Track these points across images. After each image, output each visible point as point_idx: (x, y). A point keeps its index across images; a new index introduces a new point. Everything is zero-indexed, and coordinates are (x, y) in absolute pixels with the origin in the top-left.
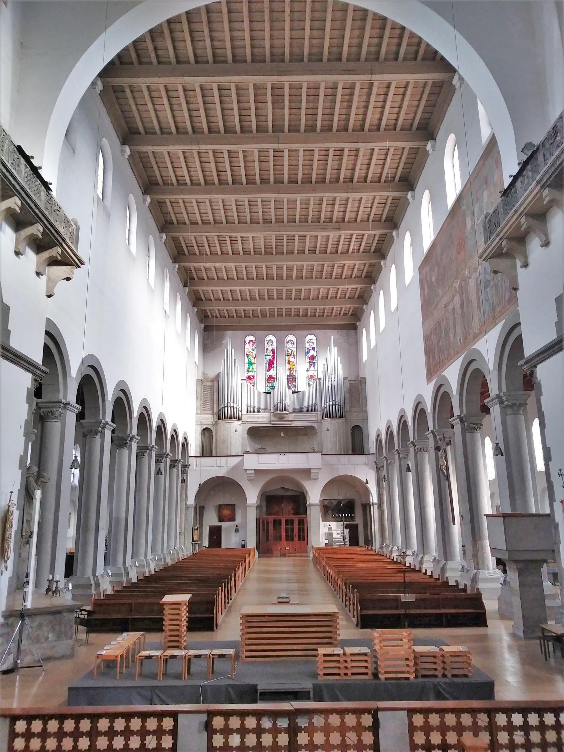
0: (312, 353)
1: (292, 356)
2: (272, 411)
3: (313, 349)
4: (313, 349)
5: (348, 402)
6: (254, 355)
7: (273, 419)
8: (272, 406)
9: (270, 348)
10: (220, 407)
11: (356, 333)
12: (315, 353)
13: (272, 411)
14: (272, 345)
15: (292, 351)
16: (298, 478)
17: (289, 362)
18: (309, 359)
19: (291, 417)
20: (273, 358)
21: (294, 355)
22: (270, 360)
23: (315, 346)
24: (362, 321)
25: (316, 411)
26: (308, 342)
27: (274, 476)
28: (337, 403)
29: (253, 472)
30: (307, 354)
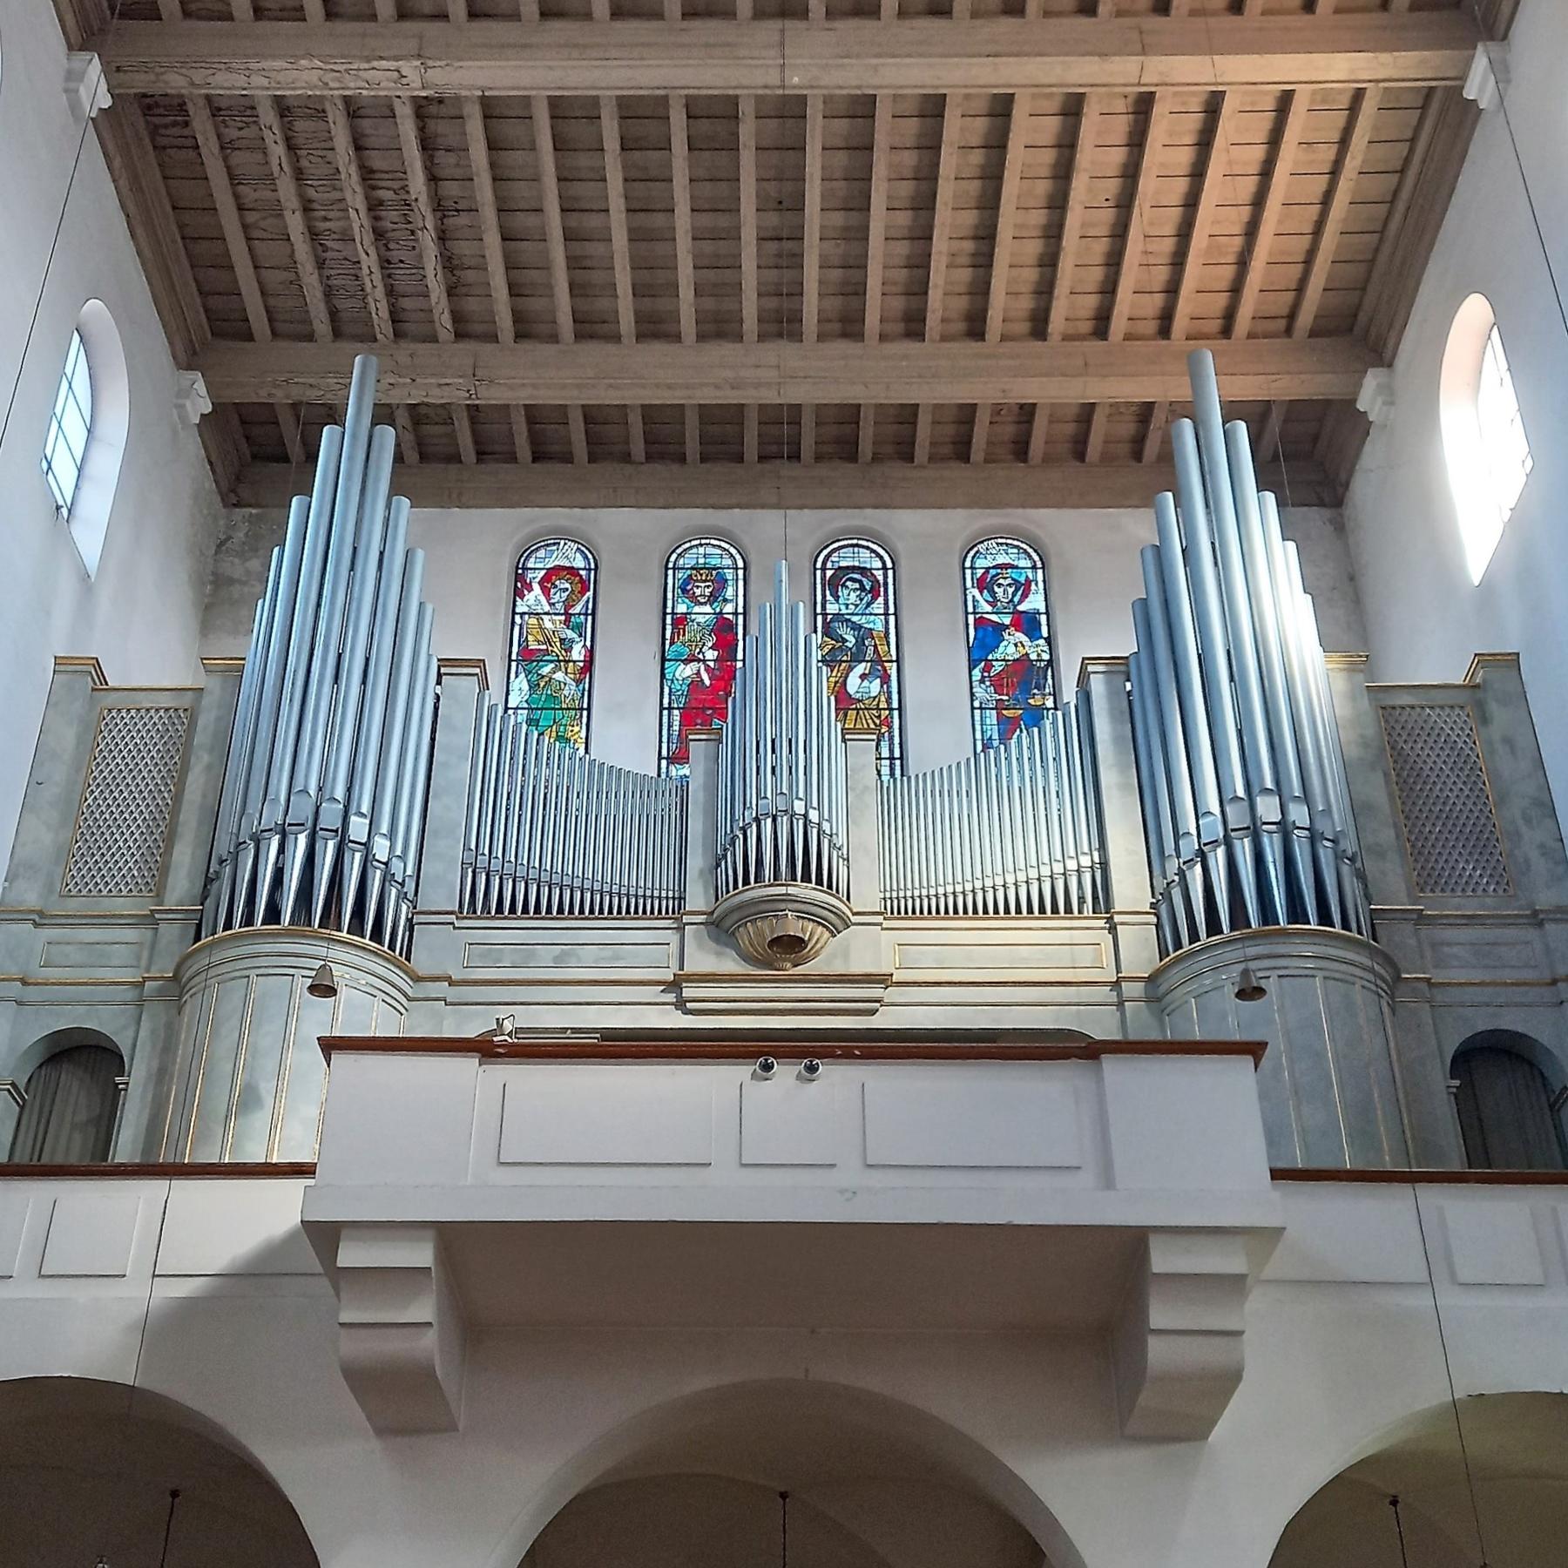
0: (1012, 646)
1: (861, 668)
2: (697, 898)
3: (1027, 624)
4: (1027, 624)
5: (1387, 836)
6: (578, 653)
7: (702, 959)
8: (696, 861)
9: (703, 614)
10: (223, 846)
11: (1340, 528)
12: (1036, 650)
13: (697, 898)
14: (712, 599)
15: (863, 634)
16: (962, 1405)
17: (844, 701)
18: (998, 684)
19: (862, 949)
20: (725, 675)
21: (878, 661)
22: (695, 684)
23: (1035, 602)
24: (1400, 363)
25: (1103, 899)
26: (982, 584)
27: (700, 1382)
28: (1299, 814)
29: (421, 1255)
30: (978, 654)
